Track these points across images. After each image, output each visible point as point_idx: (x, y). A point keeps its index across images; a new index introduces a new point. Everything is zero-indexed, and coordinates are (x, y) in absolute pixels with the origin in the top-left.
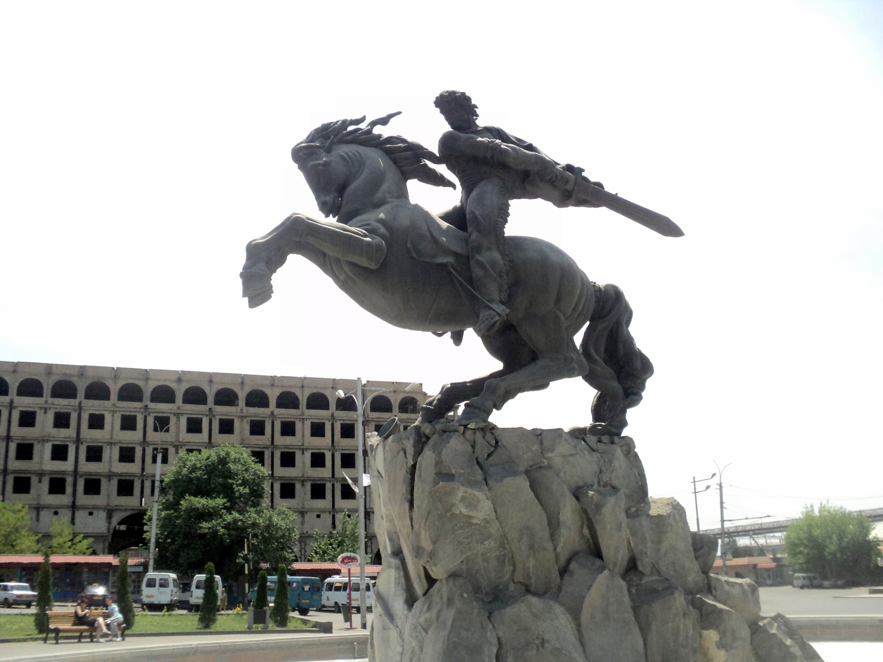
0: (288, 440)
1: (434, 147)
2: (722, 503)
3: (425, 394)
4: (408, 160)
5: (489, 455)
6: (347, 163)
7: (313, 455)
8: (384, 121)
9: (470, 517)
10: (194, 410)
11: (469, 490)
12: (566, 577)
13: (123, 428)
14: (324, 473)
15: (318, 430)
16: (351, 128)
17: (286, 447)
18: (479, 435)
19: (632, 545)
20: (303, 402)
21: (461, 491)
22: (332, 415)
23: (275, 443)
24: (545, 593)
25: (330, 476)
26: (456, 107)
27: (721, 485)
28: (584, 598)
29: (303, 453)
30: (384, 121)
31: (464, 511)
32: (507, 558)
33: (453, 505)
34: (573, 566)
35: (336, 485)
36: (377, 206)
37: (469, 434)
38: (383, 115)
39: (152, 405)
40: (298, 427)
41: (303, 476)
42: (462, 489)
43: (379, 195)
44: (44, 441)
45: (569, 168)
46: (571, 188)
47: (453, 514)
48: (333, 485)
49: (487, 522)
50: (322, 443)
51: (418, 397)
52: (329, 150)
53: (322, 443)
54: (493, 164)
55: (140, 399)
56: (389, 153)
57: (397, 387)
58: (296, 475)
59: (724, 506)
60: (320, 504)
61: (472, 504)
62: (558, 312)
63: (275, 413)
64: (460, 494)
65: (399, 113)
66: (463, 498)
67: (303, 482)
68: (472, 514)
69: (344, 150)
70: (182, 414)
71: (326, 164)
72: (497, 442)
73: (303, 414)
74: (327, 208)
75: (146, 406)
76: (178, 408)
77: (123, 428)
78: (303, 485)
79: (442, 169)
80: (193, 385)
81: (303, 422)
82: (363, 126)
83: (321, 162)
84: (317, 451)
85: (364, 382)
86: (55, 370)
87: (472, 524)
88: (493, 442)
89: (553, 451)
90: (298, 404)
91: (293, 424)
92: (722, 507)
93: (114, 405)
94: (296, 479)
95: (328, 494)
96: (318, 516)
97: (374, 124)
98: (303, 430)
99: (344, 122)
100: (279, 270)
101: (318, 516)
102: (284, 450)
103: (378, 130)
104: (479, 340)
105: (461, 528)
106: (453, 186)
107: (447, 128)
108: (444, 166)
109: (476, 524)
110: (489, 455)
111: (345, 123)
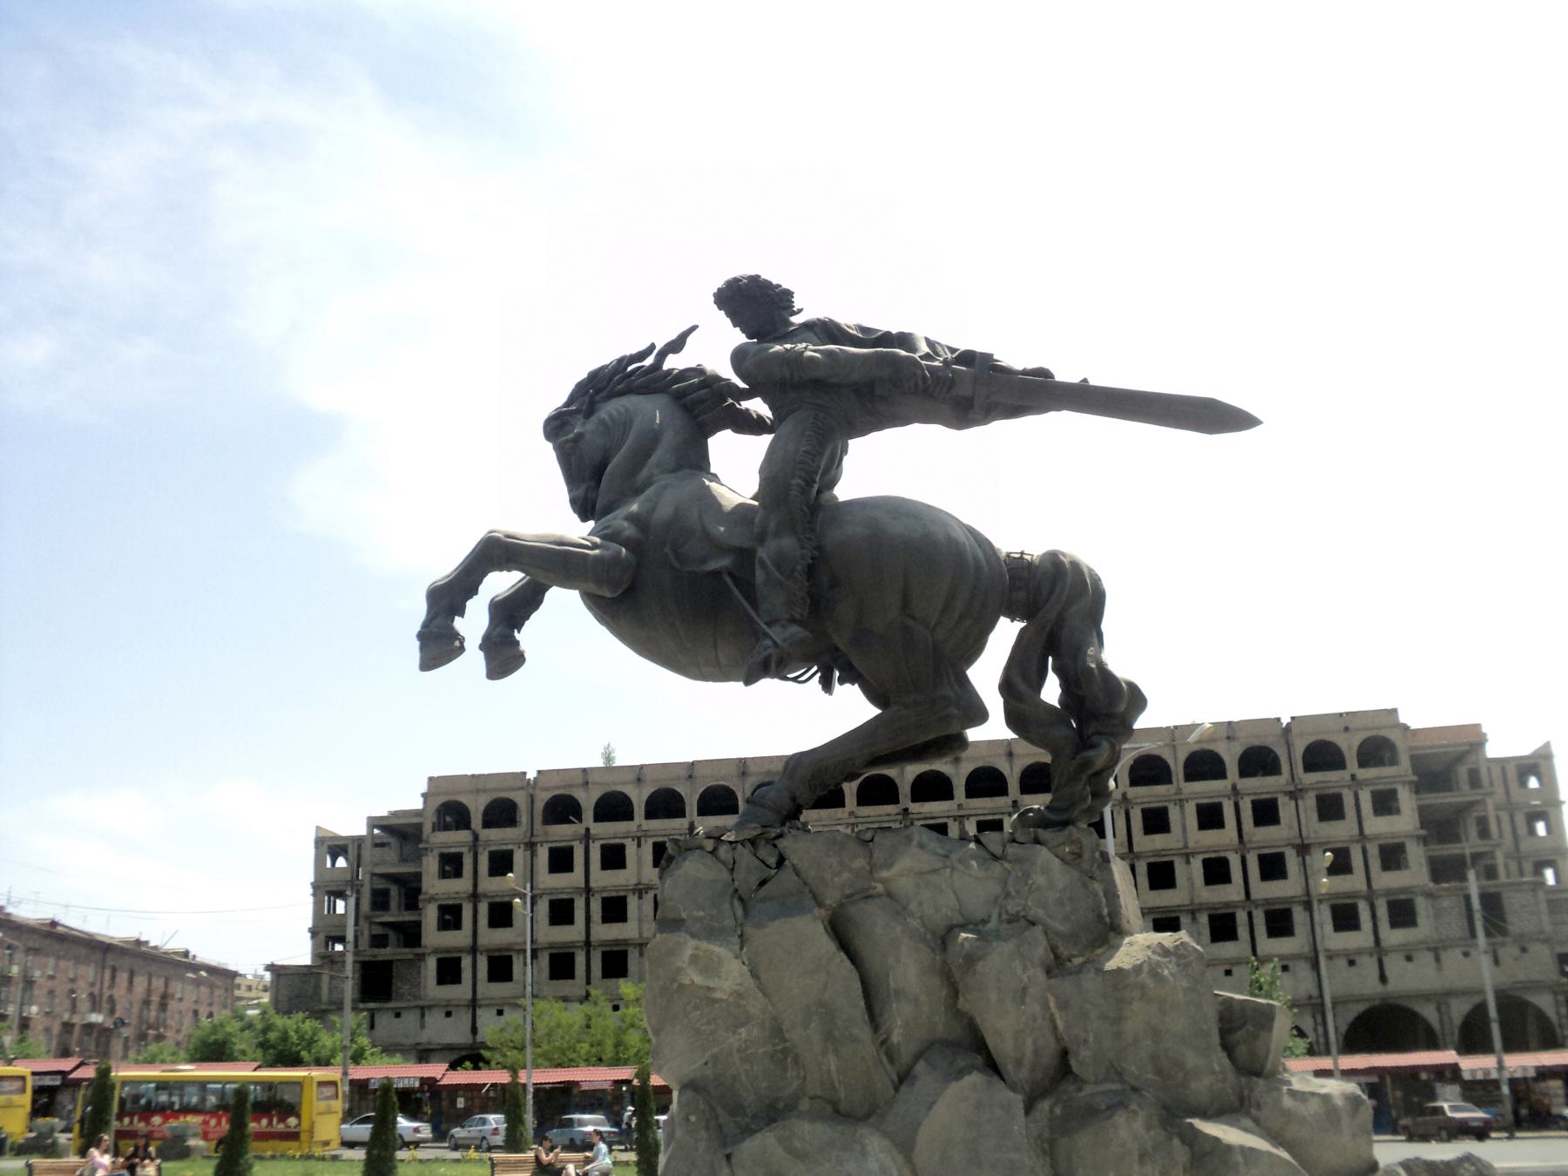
0: (1159, 841)
3: (1406, 728)
5: (763, 883)
6: (621, 427)
7: (1207, 863)
8: (677, 345)
9: (709, 989)
10: (985, 806)
11: (704, 945)
12: (904, 1088)
14: (1231, 893)
15: (1210, 817)
17: (1157, 853)
18: (744, 853)
19: (1060, 1024)
20: (1178, 770)
21: (690, 946)
22: (1234, 788)
23: (1136, 849)
24: (868, 1116)
25: (1242, 896)
28: (919, 1124)
29: (1188, 862)
30: (677, 345)
31: (698, 980)
32: (784, 1055)
33: (679, 970)
34: (921, 1067)
35: (1255, 913)
36: (638, 492)
37: (723, 851)
38: (673, 336)
39: (915, 808)
40: (1174, 815)
41: (1192, 903)
42: (692, 943)
43: (644, 473)
45: (968, 358)
46: (976, 390)
47: (681, 986)
48: (1250, 915)
49: (740, 995)
50: (1221, 840)
51: (1393, 736)
52: (590, 412)
53: (1221, 840)
55: (896, 801)
56: (679, 397)
57: (1346, 721)
58: (1179, 902)
61: (710, 967)
62: (910, 622)
63: (1129, 796)
64: (689, 952)
65: (694, 328)
66: (694, 959)
67: (1193, 913)
68: (711, 984)
69: (611, 408)
70: (968, 816)
71: (580, 436)
72: (781, 860)
73: (1179, 791)
74: (584, 509)
75: (906, 810)
76: (960, 806)
78: (1194, 919)
79: (758, 406)
80: (980, 764)
81: (1182, 807)
82: (649, 361)
83: (571, 436)
84: (1213, 855)
85: (1285, 721)
86: (752, 768)
88: (772, 861)
89: (889, 866)
90: (632, 813)
91: (622, 848)
93: (852, 814)
94: (1179, 908)
95: (1243, 931)
96: (1228, 973)
97: (663, 355)
98: (1183, 819)
99: (620, 360)
100: (534, 616)
101: (1228, 973)
102: (1152, 860)
105: (696, 1008)
107: (739, 338)
109: (721, 1000)
110: (763, 883)
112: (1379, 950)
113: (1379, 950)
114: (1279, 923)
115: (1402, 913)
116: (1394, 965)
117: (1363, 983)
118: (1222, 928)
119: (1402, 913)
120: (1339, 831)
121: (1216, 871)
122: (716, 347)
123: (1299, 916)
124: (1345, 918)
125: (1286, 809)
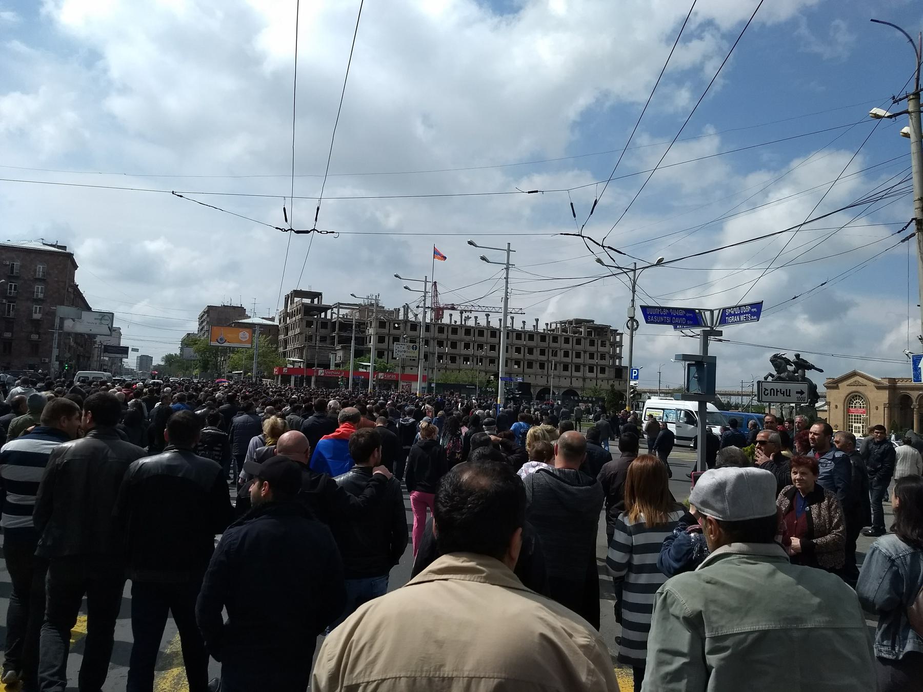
0: (555, 345)
4: (788, 362)
13: (492, 336)
14: (568, 360)
26: (797, 356)
44: (461, 341)
46: (811, 367)
50: (569, 346)
54: (802, 365)
60: (566, 373)
77: (492, 336)
112: (597, 378)
113: (597, 378)
114: (578, 369)
115: (603, 370)
116: (599, 382)
117: (565, 383)
118: (566, 368)
119: (603, 370)
120: (593, 349)
121: (566, 354)
122: (792, 358)
123: (582, 367)
124: (591, 370)
125: (583, 341)
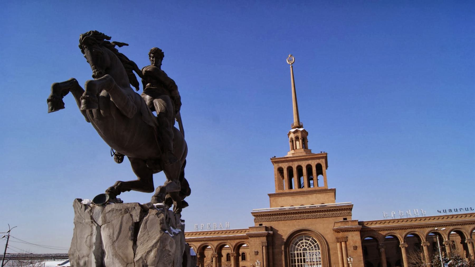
1: (140, 68)
2: (7, 245)
8: (121, 45)
9: (170, 251)
16: (105, 40)
27: (9, 237)
30: (121, 45)
59: (8, 246)
65: (128, 45)
79: (139, 80)
82: (111, 41)
87: (169, 255)
92: (6, 247)
103: (117, 47)
104: (130, 163)
105: (166, 257)
106: (138, 89)
108: (141, 79)
111: (104, 36)
